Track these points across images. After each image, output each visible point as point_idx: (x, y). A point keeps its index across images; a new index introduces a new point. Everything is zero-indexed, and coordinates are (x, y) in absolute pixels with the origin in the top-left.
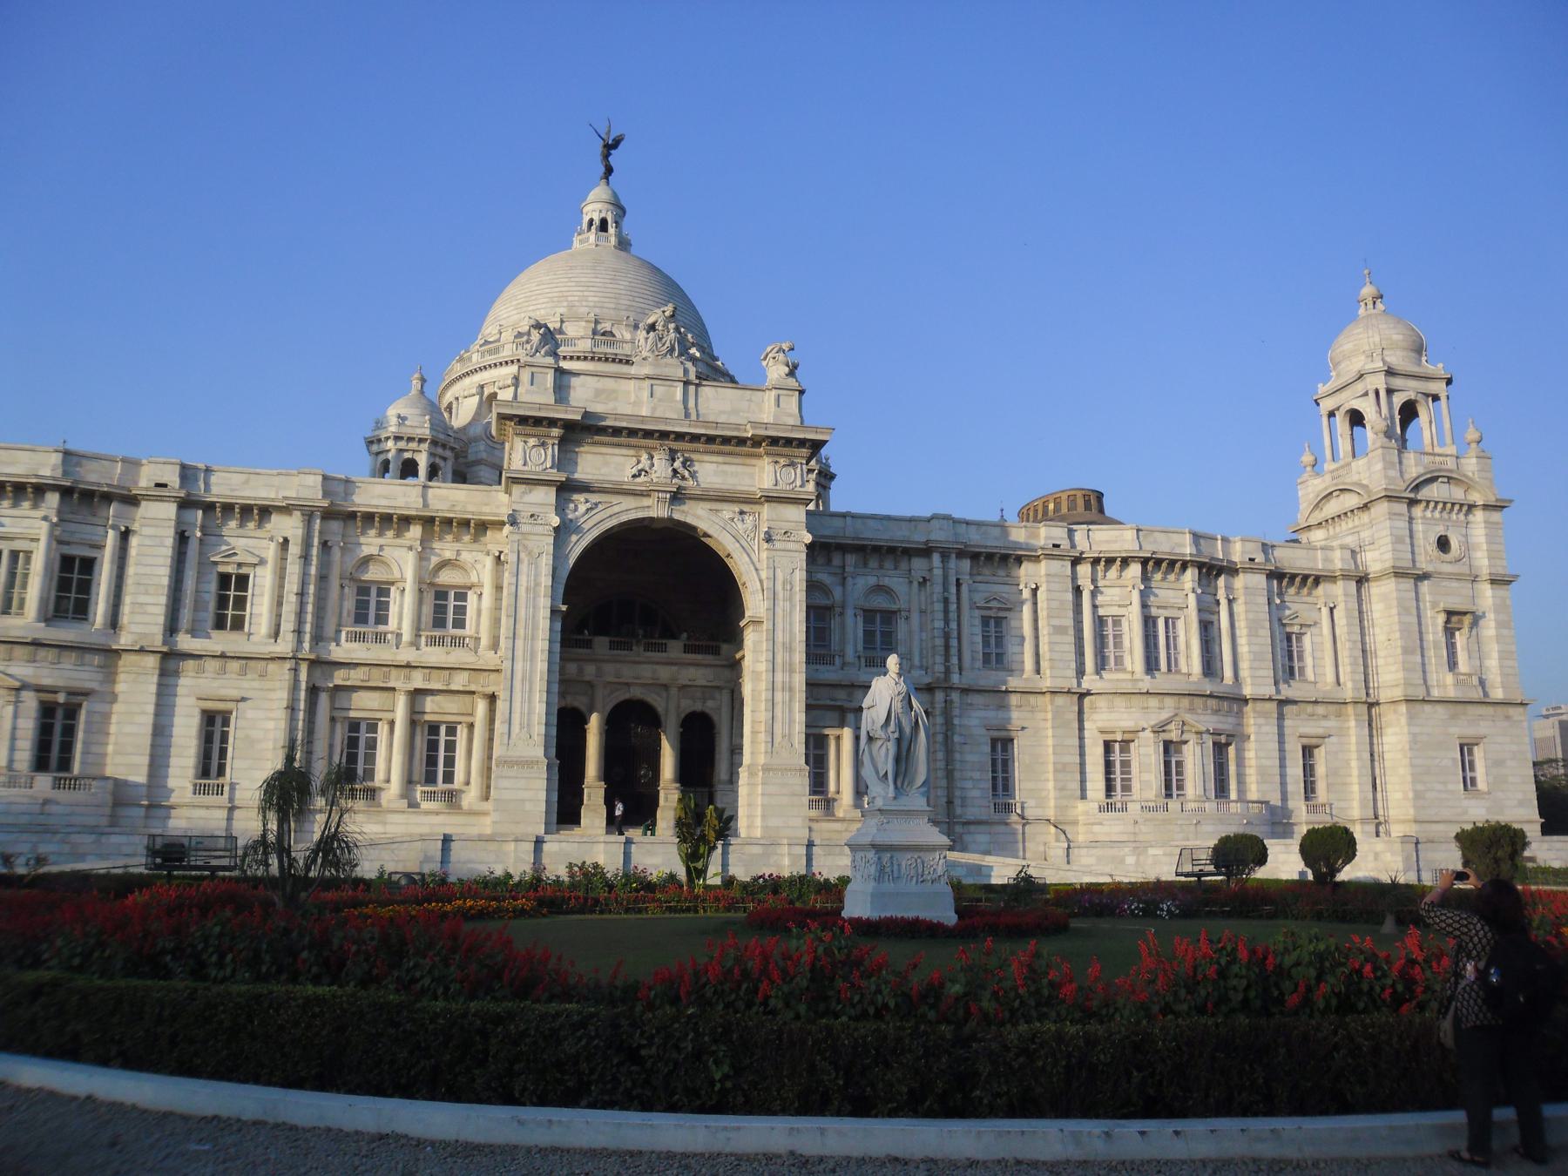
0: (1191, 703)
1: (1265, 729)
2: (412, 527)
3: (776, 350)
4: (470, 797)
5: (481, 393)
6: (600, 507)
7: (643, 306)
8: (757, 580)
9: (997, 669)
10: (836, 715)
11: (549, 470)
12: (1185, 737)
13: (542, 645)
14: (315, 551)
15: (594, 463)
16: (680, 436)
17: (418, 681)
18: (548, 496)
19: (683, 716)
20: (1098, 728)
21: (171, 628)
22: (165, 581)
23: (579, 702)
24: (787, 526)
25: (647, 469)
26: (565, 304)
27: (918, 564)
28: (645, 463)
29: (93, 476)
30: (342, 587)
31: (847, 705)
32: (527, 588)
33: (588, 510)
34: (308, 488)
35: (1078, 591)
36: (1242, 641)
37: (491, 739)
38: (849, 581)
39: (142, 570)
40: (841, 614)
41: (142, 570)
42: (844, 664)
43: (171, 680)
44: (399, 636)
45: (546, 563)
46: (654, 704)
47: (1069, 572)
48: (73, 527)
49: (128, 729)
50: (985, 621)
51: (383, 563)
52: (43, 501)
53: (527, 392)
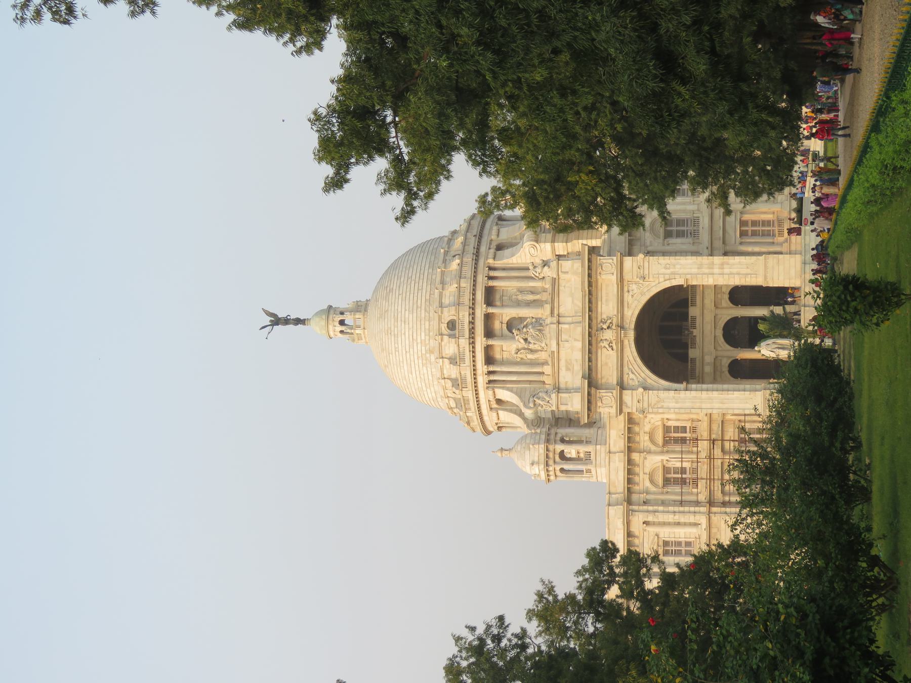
6: (631, 367)
14: (651, 508)
15: (608, 371)
16: (590, 327)
17: (718, 452)
18: (627, 396)
19: (731, 305)
23: (726, 363)
24: (635, 268)
26: (428, 355)
28: (605, 344)
30: (667, 493)
32: (677, 403)
46: (726, 320)
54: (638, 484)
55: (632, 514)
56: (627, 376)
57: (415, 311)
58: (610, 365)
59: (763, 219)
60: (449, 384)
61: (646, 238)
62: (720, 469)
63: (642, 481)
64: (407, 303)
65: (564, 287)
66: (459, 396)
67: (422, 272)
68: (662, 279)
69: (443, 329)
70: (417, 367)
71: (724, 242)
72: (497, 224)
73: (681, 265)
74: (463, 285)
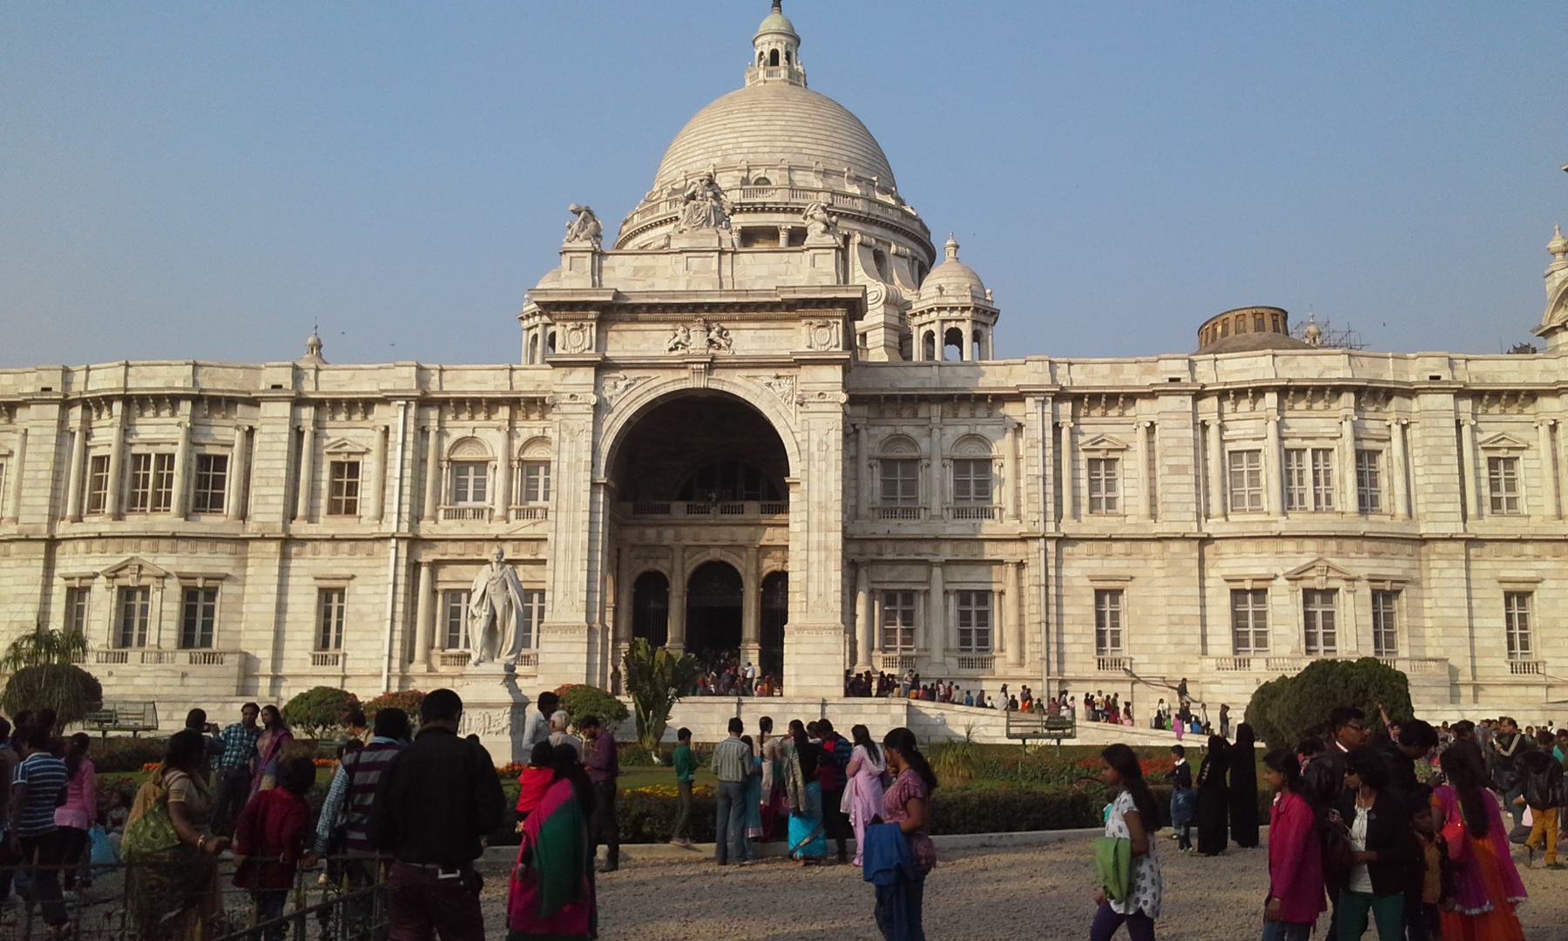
0: (1340, 546)
1: (1448, 573)
2: (500, 409)
7: (799, 145)
9: (1107, 515)
11: (587, 352)
12: (1332, 584)
14: (410, 438)
16: (713, 307)
18: (587, 375)
19: (764, 575)
20: (1222, 576)
21: (291, 515)
22: (283, 473)
23: (662, 566)
24: (821, 387)
25: (683, 341)
26: (719, 153)
28: (681, 336)
29: (217, 382)
31: (931, 558)
33: (627, 387)
34: (402, 378)
35: (1205, 427)
36: (1417, 471)
38: (936, 432)
39: (263, 465)
40: (928, 466)
41: (263, 465)
42: (932, 517)
43: (294, 563)
44: (491, 510)
45: (585, 440)
46: (736, 566)
47: (1189, 407)
48: (205, 430)
49: (257, 608)
50: (1093, 463)
51: (478, 443)
52: (179, 409)
54: (456, 418)
55: (399, 405)
56: (622, 377)
57: (784, 133)
58: (644, 346)
61: (883, 428)
62: (476, 557)
63: (457, 428)
65: (788, 262)
68: (799, 437)
69: (757, 172)
70: (704, 141)
71: (873, 562)
73: (826, 471)
74: (821, 194)
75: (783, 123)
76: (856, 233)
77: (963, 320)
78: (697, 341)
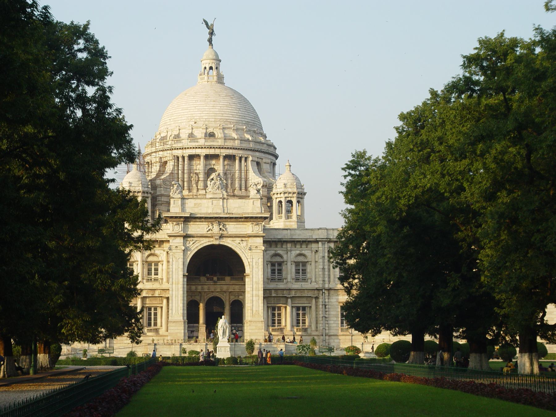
3: (253, 185)
4: (162, 331)
5: (160, 162)
6: (197, 242)
8: (247, 262)
10: (284, 299)
13: (180, 286)
15: (194, 228)
16: (221, 218)
18: (181, 240)
23: (197, 298)
25: (211, 229)
26: (193, 120)
27: (314, 246)
28: (211, 227)
33: (193, 243)
37: (168, 312)
38: (289, 253)
46: (222, 298)
53: (173, 207)
57: (220, 113)
59: (282, 320)
60: (177, 133)
64: (225, 108)
65: (245, 203)
66: (168, 139)
67: (243, 117)
70: (186, 113)
72: (271, 162)
73: (258, 271)
75: (219, 108)
76: (250, 156)
77: (294, 197)
78: (216, 228)
